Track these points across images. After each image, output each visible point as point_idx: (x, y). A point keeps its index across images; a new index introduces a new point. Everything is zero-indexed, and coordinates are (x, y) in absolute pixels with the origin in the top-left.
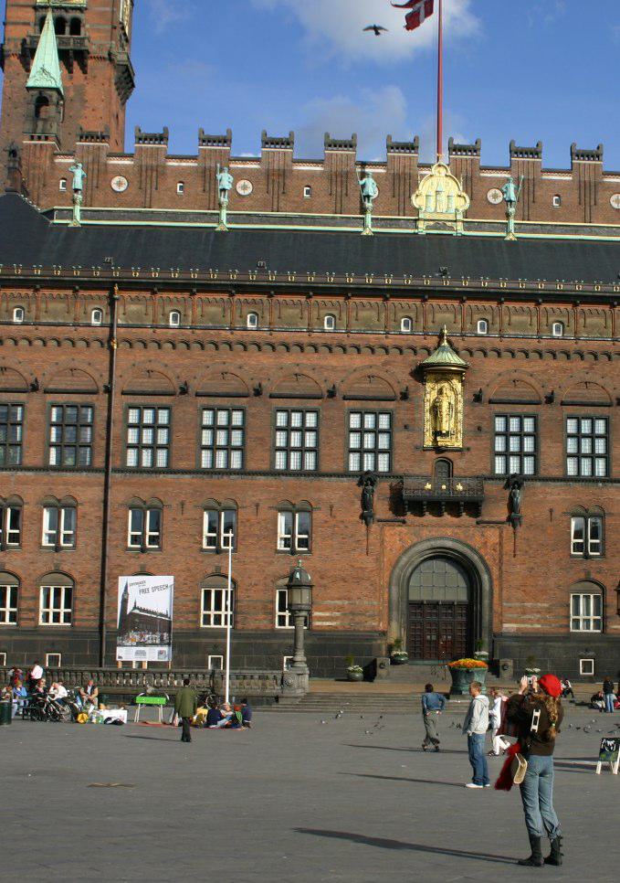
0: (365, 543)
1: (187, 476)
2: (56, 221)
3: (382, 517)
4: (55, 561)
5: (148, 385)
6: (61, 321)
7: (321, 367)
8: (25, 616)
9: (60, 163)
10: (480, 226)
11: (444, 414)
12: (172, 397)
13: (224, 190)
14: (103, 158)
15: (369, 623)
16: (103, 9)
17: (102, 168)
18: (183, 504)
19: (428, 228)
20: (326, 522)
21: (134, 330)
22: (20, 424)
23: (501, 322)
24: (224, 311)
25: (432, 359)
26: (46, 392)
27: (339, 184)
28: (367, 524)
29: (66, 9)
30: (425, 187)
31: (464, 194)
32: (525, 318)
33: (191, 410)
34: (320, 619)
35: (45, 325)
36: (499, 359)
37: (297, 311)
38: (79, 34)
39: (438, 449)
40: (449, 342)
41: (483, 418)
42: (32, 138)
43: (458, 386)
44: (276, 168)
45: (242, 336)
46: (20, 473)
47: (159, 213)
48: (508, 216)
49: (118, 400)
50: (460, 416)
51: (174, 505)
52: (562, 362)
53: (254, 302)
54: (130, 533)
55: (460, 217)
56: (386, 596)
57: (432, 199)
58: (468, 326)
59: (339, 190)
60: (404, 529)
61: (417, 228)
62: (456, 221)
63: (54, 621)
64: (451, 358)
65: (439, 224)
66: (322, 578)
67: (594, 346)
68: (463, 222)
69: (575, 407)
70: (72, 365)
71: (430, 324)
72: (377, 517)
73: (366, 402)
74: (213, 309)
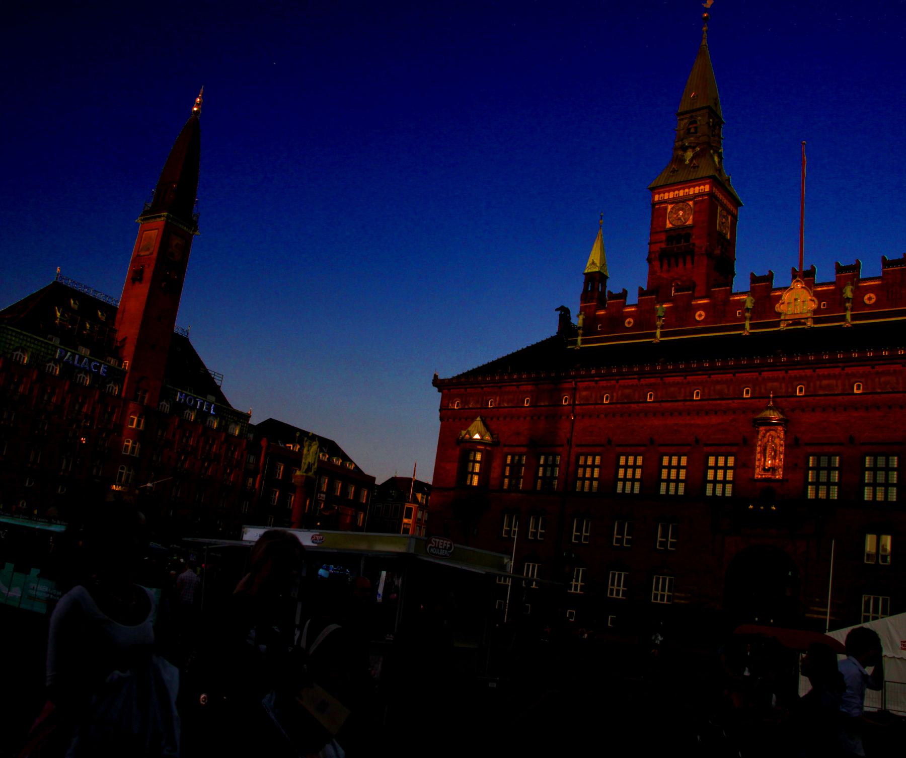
19: (788, 325)
30: (786, 297)
31: (813, 298)
32: (833, 382)
43: (782, 436)
50: (782, 456)
58: (790, 390)
62: (807, 318)
65: (796, 322)
71: (763, 391)
74: (627, 391)
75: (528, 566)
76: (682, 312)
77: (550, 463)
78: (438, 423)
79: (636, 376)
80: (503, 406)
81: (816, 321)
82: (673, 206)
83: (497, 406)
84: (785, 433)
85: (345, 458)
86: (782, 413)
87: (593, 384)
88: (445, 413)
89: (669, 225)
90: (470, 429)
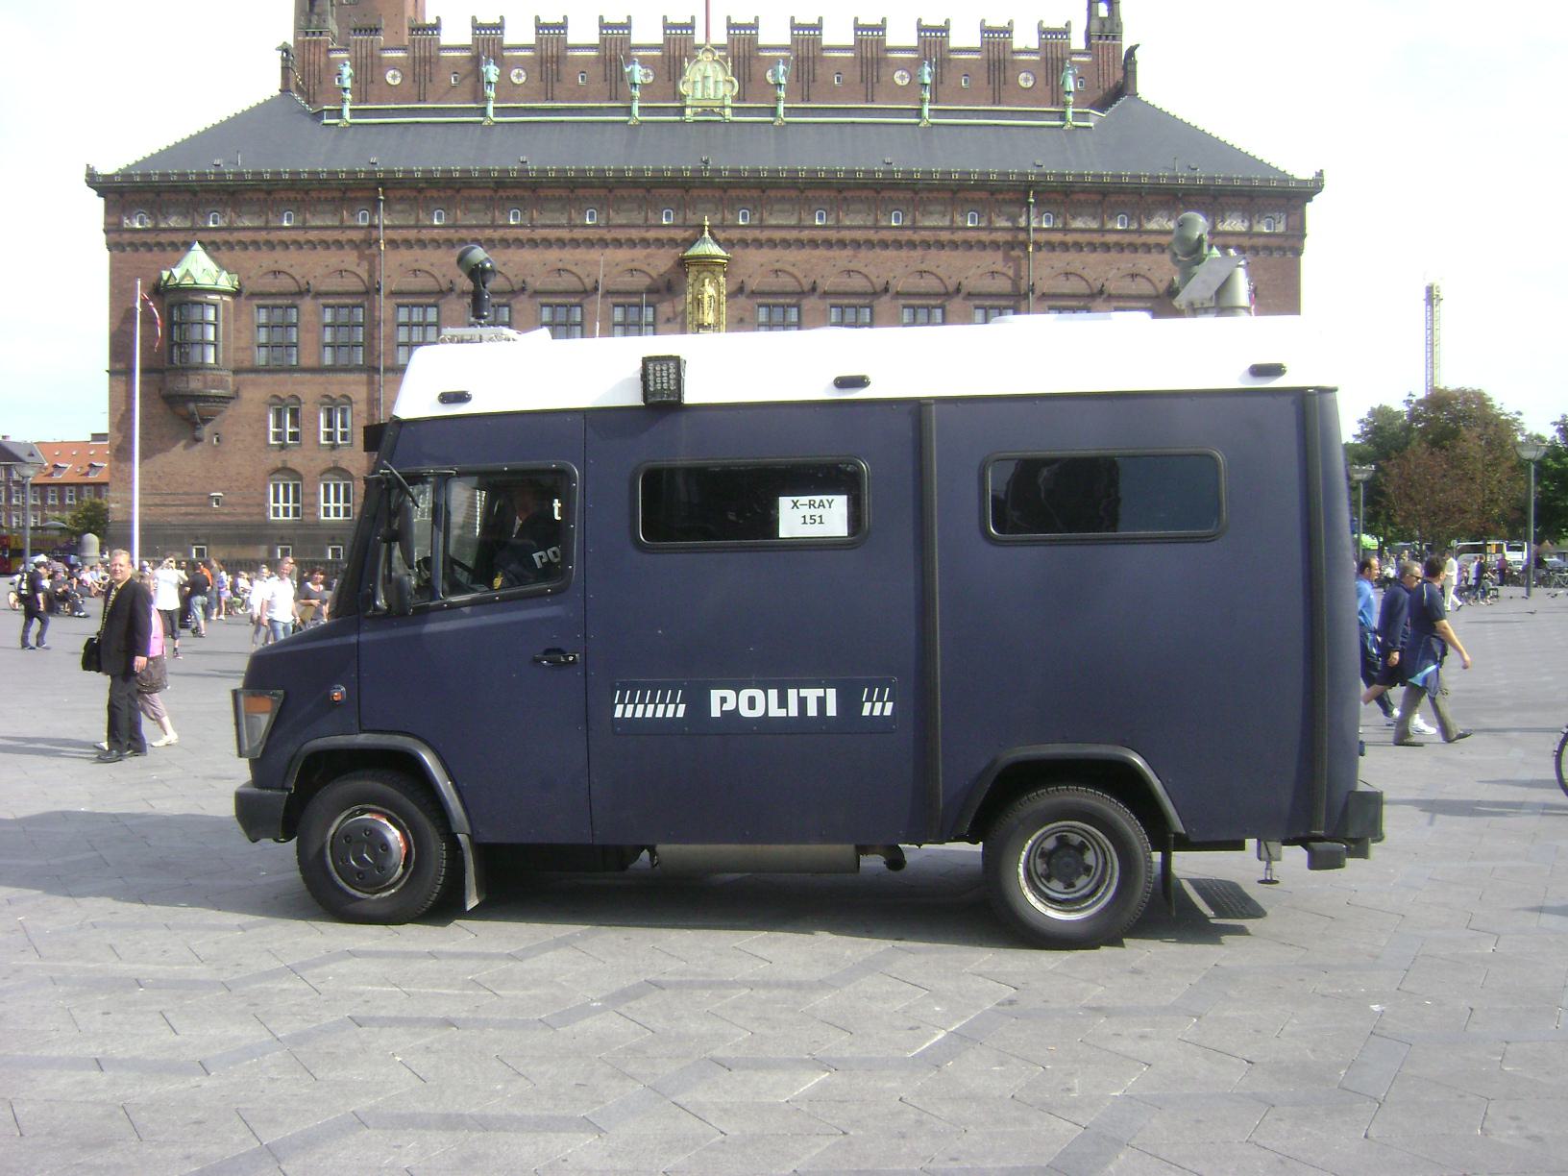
2: (326, 121)
4: (334, 458)
6: (330, 223)
8: (308, 511)
9: (335, 58)
10: (748, 111)
11: (706, 306)
14: (376, 52)
17: (376, 61)
19: (696, 114)
22: (295, 325)
25: (692, 252)
31: (734, 79)
33: (458, 307)
40: (710, 233)
43: (722, 279)
44: (549, 54)
45: (505, 233)
48: (778, 99)
50: (724, 308)
52: (822, 252)
55: (728, 102)
57: (699, 86)
62: (724, 107)
63: (335, 516)
64: (711, 249)
65: (707, 111)
68: (732, 107)
70: (343, 266)
75: (327, 487)
78: (104, 256)
81: (736, 111)
88: (117, 239)
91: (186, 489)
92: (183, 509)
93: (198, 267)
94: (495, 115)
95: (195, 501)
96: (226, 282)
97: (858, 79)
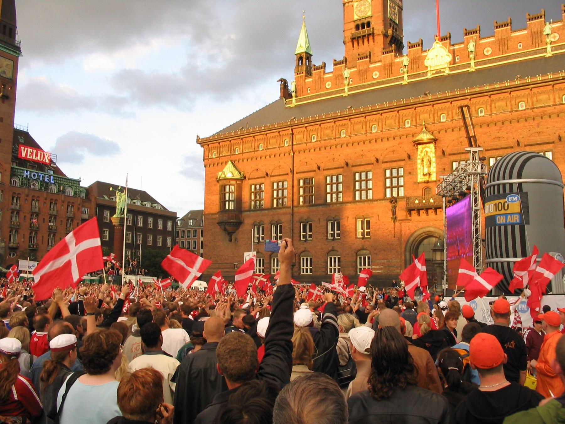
0: (393, 232)
1: (321, 207)
2: (287, 106)
3: (401, 219)
5: (306, 168)
7: (372, 150)
10: (458, 68)
12: (314, 173)
13: (346, 78)
15: (395, 272)
16: (378, 14)
18: (319, 220)
20: (376, 223)
21: (299, 146)
23: (452, 114)
24: (332, 131)
26: (271, 176)
27: (415, 63)
28: (394, 222)
29: (365, 18)
34: (375, 269)
35: (269, 149)
36: (453, 133)
37: (360, 126)
38: (370, 27)
39: (425, 182)
41: (445, 164)
42: (298, 74)
44: (388, 63)
45: (339, 141)
46: (263, 212)
47: (323, 94)
49: (296, 176)
51: (316, 220)
53: (342, 125)
54: (302, 233)
56: (403, 257)
59: (415, 66)
60: (411, 224)
61: (427, 75)
62: (445, 68)
66: (375, 250)
67: (501, 117)
68: (449, 67)
69: (492, 151)
71: (418, 121)
72: (398, 218)
73: (394, 163)
76: (363, 74)
77: (280, 187)
79: (332, 120)
80: (245, 152)
82: (357, 3)
83: (241, 152)
84: (436, 148)
85: (153, 201)
86: (432, 134)
87: (304, 129)
88: (208, 162)
89: (356, 17)
90: (224, 170)
91: (226, 261)
92: (225, 270)
93: (229, 172)
94: (349, 91)
95: (229, 267)
96: (237, 176)
97: (531, 43)
